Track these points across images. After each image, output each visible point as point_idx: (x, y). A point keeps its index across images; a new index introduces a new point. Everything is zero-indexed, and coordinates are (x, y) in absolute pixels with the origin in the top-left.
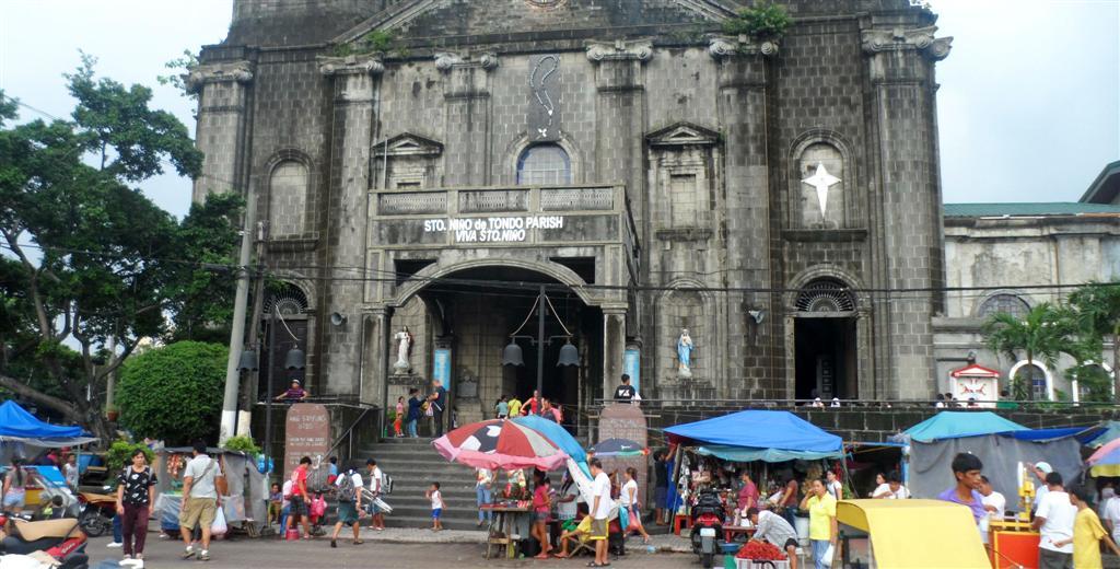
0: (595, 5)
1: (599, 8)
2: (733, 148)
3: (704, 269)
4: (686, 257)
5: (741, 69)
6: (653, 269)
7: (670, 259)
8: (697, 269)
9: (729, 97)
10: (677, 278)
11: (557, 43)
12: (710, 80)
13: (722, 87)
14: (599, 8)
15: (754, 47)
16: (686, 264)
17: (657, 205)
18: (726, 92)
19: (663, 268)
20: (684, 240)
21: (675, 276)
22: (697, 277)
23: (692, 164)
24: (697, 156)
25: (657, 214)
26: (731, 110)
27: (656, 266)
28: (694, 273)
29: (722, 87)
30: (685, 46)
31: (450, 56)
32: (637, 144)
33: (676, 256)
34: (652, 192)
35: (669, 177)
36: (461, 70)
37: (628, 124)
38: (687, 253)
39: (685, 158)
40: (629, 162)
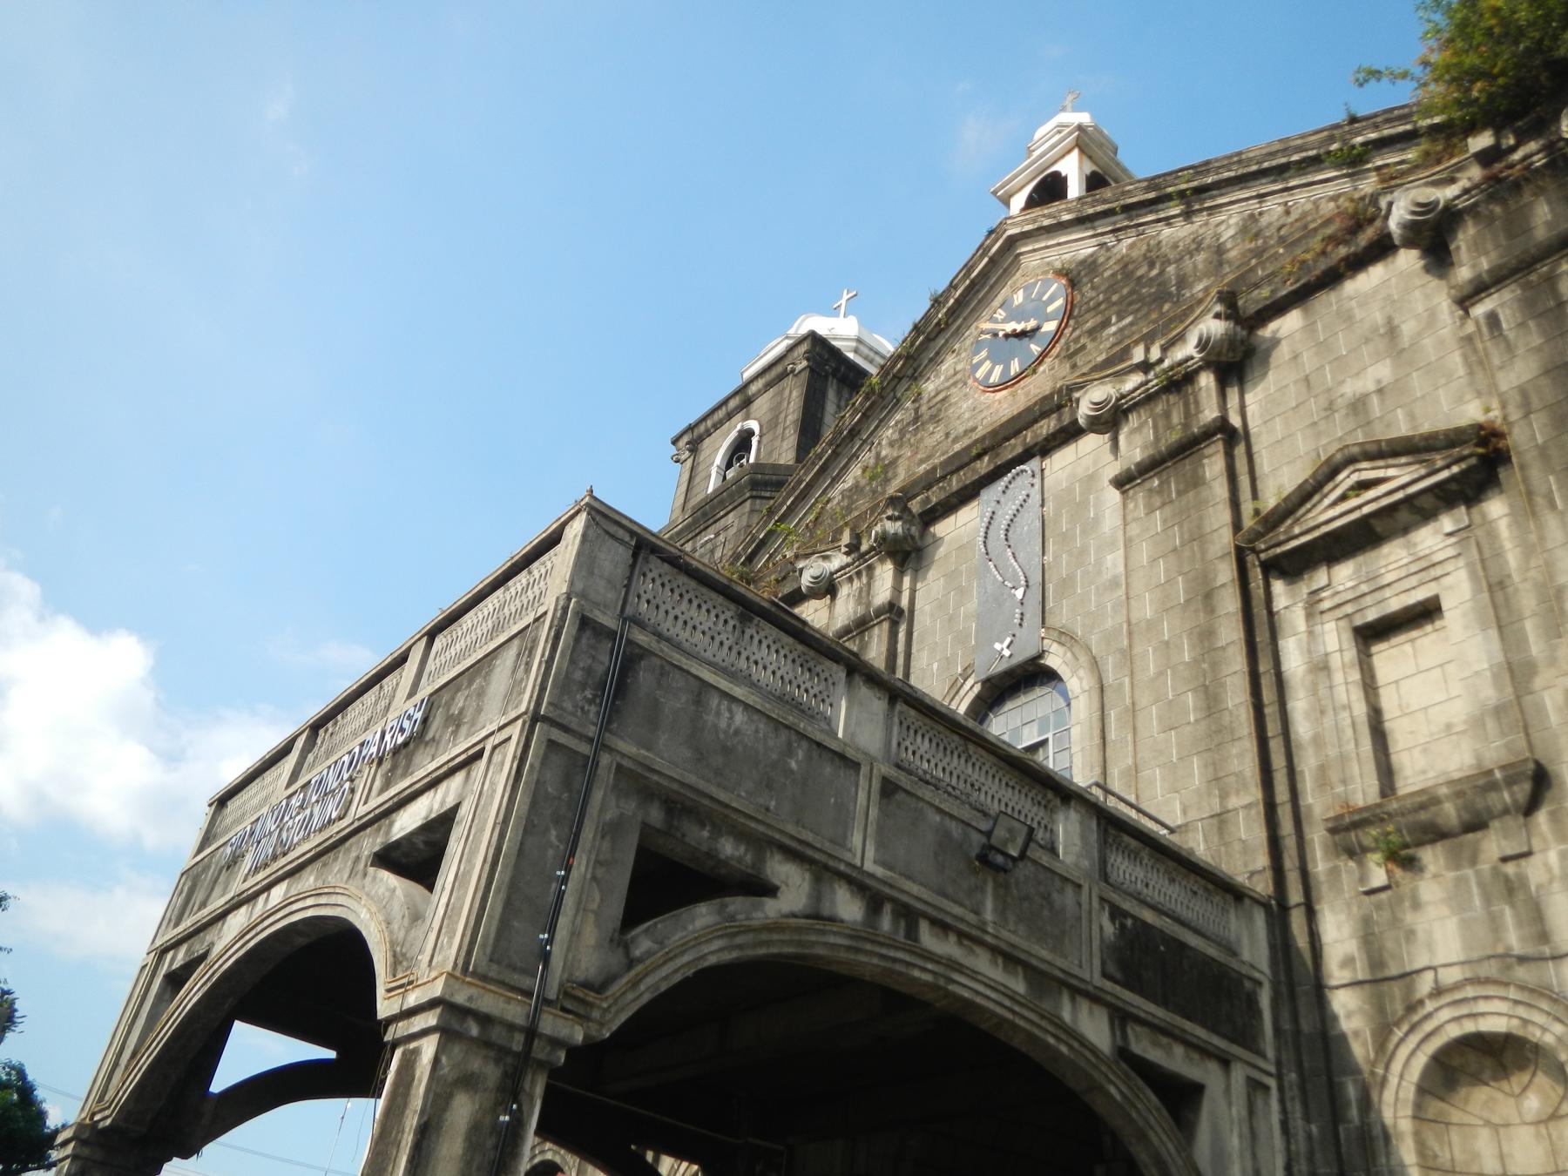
0: (1120, 319)
1: (1129, 319)
2: (1543, 452)
3: (1544, 936)
4: (1458, 900)
5: (1516, 226)
6: (1336, 973)
7: (1396, 922)
8: (1514, 940)
9: (1493, 320)
10: (1438, 992)
11: (1029, 436)
12: (1432, 314)
13: (1465, 301)
14: (1129, 319)
15: (1533, 146)
16: (1466, 925)
17: (1318, 741)
18: (1479, 310)
19: (1376, 961)
20: (1435, 834)
21: (1425, 984)
22: (1521, 973)
23: (1427, 567)
24: (1432, 538)
25: (1322, 769)
26: (1509, 348)
27: (1348, 962)
28: (1508, 959)
29: (1465, 301)
30: (1332, 278)
31: (826, 558)
32: (1226, 573)
33: (1416, 905)
34: (1299, 705)
35: (1348, 639)
36: (850, 579)
37: (1198, 537)
38: (1461, 882)
39: (1392, 557)
40: (1206, 636)
